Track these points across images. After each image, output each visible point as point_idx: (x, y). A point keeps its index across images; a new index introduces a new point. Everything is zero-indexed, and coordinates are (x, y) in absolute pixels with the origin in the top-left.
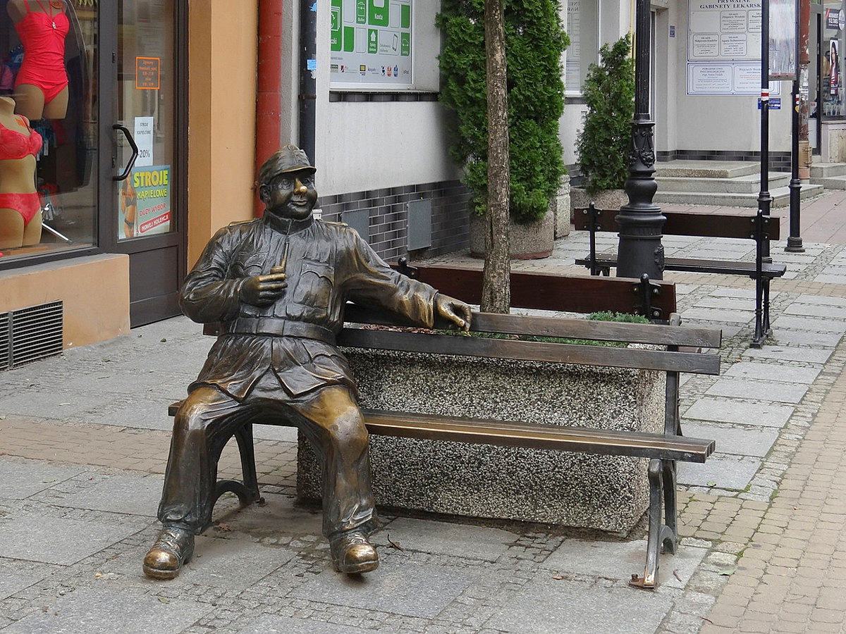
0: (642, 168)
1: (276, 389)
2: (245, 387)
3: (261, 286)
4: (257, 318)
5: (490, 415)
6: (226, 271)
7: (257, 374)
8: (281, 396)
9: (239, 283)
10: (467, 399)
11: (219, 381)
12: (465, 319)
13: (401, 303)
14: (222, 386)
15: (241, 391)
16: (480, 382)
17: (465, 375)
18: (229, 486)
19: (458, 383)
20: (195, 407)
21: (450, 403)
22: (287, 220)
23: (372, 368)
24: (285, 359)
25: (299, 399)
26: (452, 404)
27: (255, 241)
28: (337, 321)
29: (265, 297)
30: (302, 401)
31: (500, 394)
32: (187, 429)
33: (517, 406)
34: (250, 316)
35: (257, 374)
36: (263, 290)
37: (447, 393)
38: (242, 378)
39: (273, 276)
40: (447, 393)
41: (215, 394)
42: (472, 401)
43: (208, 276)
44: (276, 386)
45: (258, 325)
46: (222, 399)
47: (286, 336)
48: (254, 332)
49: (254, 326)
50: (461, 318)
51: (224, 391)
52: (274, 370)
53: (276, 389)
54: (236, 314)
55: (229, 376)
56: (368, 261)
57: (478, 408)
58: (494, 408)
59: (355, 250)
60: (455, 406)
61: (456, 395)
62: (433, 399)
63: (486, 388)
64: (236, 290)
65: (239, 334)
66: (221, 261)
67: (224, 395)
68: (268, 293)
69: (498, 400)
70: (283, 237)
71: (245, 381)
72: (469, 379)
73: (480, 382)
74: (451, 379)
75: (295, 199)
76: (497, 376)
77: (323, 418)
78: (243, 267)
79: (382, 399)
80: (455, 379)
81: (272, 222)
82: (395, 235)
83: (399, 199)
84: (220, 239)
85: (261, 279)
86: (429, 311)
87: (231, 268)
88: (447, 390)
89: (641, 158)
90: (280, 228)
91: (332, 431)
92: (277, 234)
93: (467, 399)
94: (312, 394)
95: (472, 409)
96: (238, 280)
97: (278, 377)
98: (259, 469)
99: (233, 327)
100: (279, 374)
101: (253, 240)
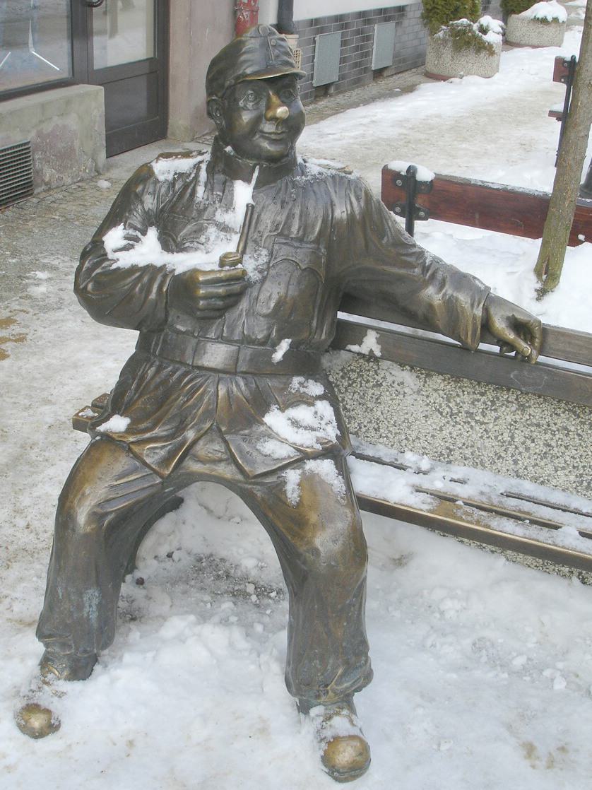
1: (220, 461)
5: (538, 462)
10: (506, 435)
12: (532, 345)
13: (431, 306)
15: (165, 461)
16: (530, 415)
17: (508, 402)
19: (496, 410)
20: (87, 492)
21: (480, 435)
23: (369, 370)
26: (481, 437)
28: (326, 339)
31: (558, 436)
32: (74, 530)
33: (581, 456)
36: (205, 297)
37: (477, 422)
40: (477, 422)
42: (512, 437)
44: (224, 457)
46: (135, 470)
47: (242, 372)
49: (189, 352)
50: (525, 340)
52: (220, 430)
53: (220, 461)
57: (521, 449)
58: (545, 453)
59: (363, 218)
60: (487, 441)
61: (491, 426)
62: (454, 426)
63: (538, 425)
64: (160, 287)
69: (553, 444)
71: (169, 445)
72: (514, 409)
73: (530, 415)
74: (485, 403)
76: (558, 411)
79: (379, 413)
80: (492, 406)
82: (362, 56)
83: (368, 22)
86: (474, 325)
88: (477, 418)
91: (310, 557)
93: (506, 435)
95: (511, 449)
97: (226, 442)
99: (157, 344)
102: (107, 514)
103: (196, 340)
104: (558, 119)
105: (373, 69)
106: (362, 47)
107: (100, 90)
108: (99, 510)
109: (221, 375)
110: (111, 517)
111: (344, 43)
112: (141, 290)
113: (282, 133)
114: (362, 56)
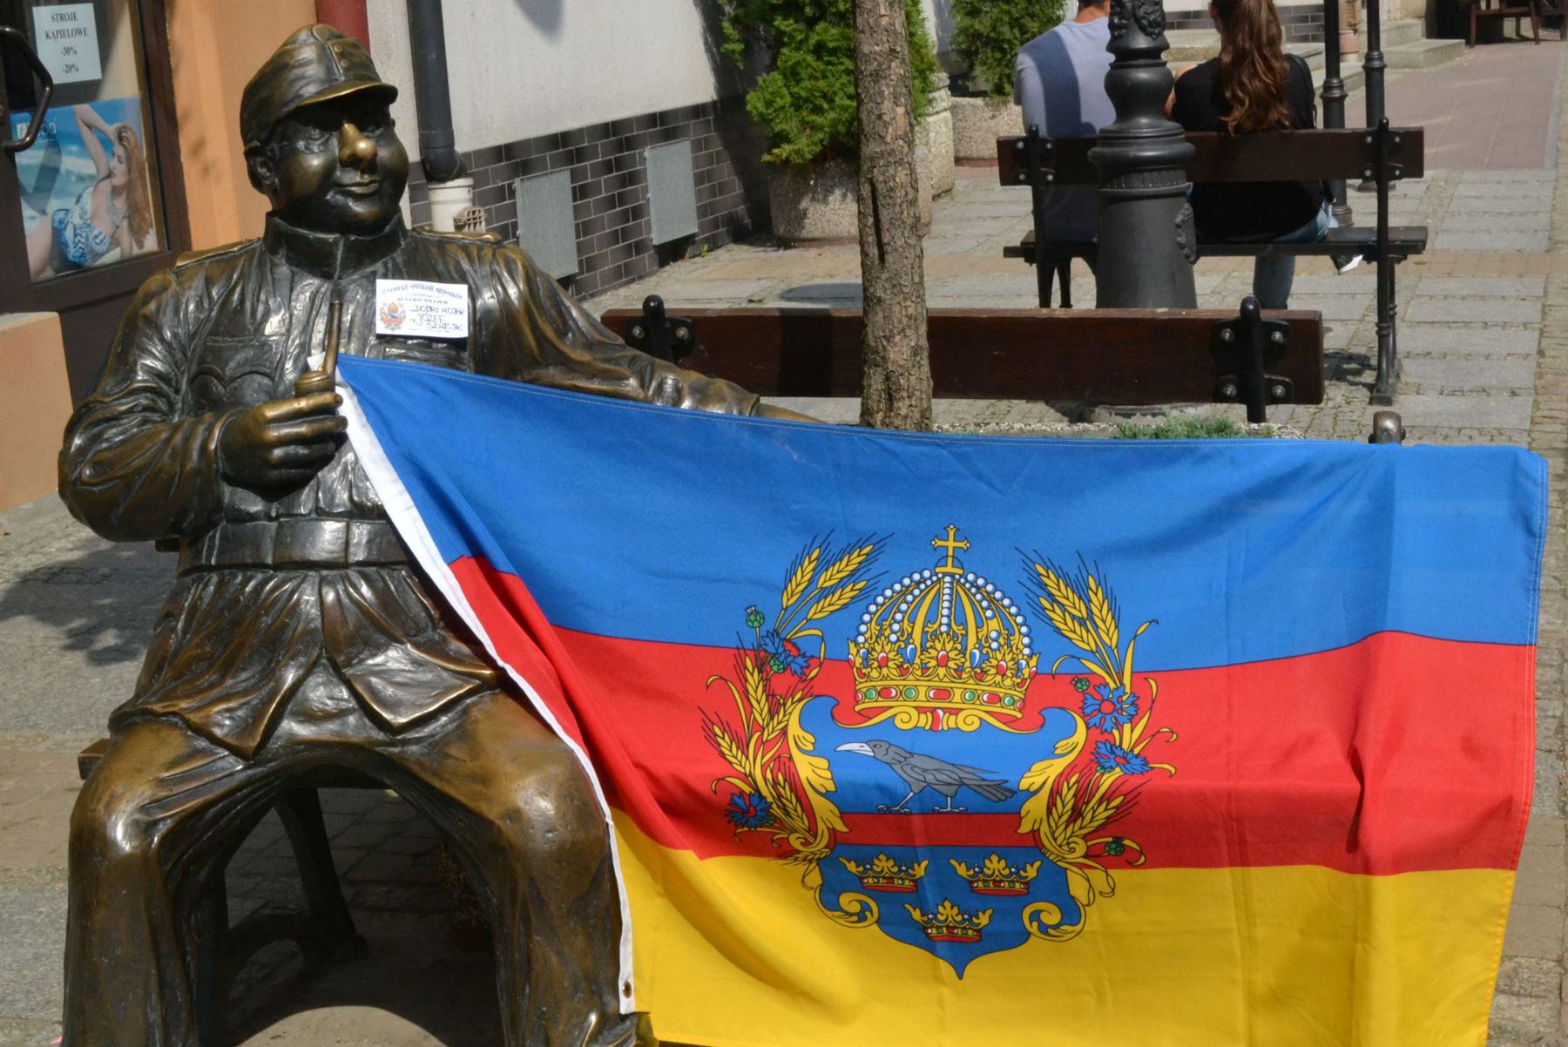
0: (1141, 42)
1: (342, 714)
2: (257, 714)
3: (274, 433)
4: (271, 519)
6: (177, 391)
7: (290, 677)
8: (354, 727)
9: (210, 429)
11: (183, 705)
14: (195, 718)
15: (245, 728)
18: (259, 930)
22: (331, 237)
24: (359, 627)
25: (409, 735)
27: (248, 305)
29: (286, 462)
30: (418, 741)
34: (253, 517)
35: (290, 677)
36: (282, 442)
38: (246, 692)
39: (303, 404)
41: (175, 743)
43: (130, 411)
45: (278, 541)
46: (196, 753)
47: (359, 564)
48: (269, 560)
51: (202, 731)
54: (214, 512)
55: (212, 686)
56: (562, 334)
65: (230, 566)
66: (159, 365)
67: (202, 743)
68: (291, 449)
70: (326, 287)
71: (254, 699)
75: (351, 177)
77: (479, 787)
78: (220, 378)
81: (290, 248)
82: (625, 217)
83: (630, 144)
84: (152, 306)
85: (271, 413)
87: (191, 381)
89: (1138, 21)
90: (315, 262)
91: (506, 826)
92: (309, 286)
94: (444, 719)
96: (208, 416)
98: (341, 858)
99: (211, 549)
100: (349, 672)
101: (242, 301)
102: (155, 823)
103: (274, 525)
104: (1029, 260)
105: (656, 242)
106: (622, 199)
107: (55, 315)
108: (145, 818)
109: (324, 572)
110: (163, 828)
111: (580, 193)
112: (173, 456)
113: (372, 182)
114: (625, 217)
